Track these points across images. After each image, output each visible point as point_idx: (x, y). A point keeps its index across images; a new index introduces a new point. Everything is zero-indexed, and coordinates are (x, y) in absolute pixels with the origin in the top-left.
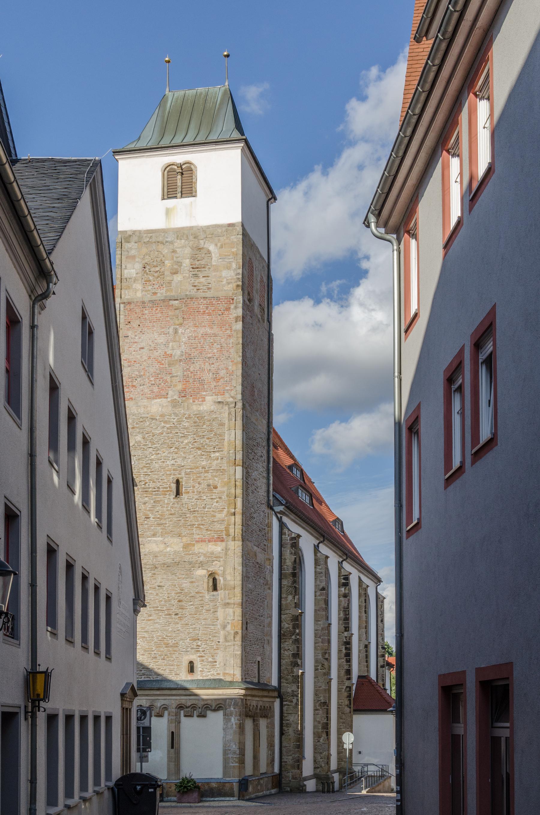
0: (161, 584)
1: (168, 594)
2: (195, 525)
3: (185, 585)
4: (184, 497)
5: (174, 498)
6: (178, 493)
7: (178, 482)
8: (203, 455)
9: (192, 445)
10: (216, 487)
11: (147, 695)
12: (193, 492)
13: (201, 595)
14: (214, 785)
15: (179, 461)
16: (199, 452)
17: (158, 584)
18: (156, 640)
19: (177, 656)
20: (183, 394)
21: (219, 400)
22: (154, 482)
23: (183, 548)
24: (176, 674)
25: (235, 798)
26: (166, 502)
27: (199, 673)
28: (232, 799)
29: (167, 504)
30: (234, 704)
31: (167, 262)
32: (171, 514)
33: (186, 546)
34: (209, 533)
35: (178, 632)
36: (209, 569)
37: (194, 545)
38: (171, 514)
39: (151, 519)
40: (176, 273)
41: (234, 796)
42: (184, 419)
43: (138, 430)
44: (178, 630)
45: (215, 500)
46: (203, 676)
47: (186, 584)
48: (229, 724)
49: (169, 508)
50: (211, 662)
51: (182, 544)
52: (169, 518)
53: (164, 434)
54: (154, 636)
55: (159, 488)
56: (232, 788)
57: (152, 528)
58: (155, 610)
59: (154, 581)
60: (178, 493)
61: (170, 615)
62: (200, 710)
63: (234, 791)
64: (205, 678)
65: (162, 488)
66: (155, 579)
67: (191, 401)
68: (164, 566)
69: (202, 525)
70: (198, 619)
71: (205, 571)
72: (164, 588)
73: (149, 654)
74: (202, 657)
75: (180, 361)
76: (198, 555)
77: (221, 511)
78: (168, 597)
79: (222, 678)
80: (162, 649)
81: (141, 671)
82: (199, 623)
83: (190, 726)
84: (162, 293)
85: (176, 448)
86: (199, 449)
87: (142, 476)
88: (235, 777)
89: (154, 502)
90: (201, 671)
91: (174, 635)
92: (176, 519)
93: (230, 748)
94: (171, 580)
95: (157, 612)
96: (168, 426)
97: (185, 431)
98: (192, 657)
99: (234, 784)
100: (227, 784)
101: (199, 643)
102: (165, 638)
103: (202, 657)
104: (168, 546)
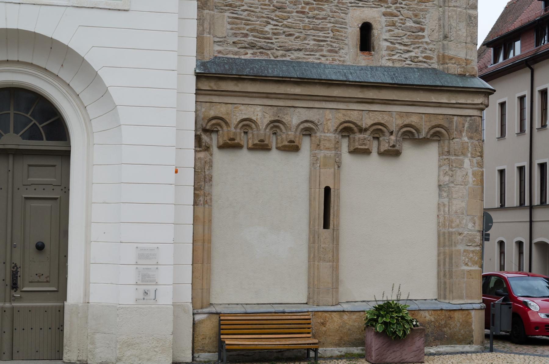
11: (268, 96)
14: (428, 317)
19: (334, 9)
24: (330, 51)
25: (474, 347)
27: (384, 53)
28: (467, 348)
30: (470, 127)
41: (471, 343)
46: (393, 61)
48: (459, 174)
50: (411, 30)
56: (467, 324)
62: (393, 138)
63: (471, 331)
64: (397, 65)
74: (392, 15)
79: (435, 66)
81: (246, 35)
83: (364, 180)
88: (472, 298)
90: (388, 48)
93: (460, 230)
98: (371, 14)
99: (473, 313)
100: (457, 315)
103: (392, 15)
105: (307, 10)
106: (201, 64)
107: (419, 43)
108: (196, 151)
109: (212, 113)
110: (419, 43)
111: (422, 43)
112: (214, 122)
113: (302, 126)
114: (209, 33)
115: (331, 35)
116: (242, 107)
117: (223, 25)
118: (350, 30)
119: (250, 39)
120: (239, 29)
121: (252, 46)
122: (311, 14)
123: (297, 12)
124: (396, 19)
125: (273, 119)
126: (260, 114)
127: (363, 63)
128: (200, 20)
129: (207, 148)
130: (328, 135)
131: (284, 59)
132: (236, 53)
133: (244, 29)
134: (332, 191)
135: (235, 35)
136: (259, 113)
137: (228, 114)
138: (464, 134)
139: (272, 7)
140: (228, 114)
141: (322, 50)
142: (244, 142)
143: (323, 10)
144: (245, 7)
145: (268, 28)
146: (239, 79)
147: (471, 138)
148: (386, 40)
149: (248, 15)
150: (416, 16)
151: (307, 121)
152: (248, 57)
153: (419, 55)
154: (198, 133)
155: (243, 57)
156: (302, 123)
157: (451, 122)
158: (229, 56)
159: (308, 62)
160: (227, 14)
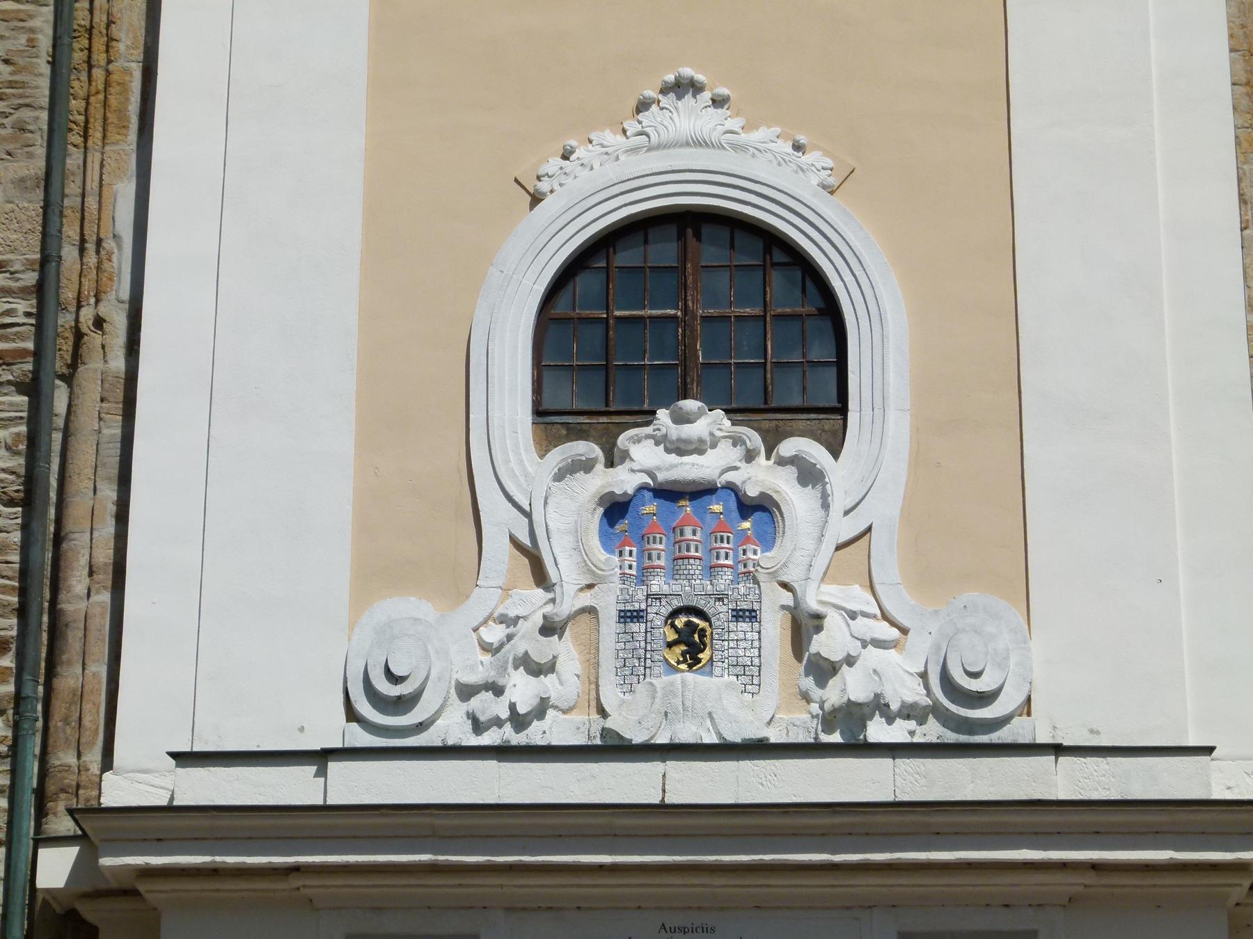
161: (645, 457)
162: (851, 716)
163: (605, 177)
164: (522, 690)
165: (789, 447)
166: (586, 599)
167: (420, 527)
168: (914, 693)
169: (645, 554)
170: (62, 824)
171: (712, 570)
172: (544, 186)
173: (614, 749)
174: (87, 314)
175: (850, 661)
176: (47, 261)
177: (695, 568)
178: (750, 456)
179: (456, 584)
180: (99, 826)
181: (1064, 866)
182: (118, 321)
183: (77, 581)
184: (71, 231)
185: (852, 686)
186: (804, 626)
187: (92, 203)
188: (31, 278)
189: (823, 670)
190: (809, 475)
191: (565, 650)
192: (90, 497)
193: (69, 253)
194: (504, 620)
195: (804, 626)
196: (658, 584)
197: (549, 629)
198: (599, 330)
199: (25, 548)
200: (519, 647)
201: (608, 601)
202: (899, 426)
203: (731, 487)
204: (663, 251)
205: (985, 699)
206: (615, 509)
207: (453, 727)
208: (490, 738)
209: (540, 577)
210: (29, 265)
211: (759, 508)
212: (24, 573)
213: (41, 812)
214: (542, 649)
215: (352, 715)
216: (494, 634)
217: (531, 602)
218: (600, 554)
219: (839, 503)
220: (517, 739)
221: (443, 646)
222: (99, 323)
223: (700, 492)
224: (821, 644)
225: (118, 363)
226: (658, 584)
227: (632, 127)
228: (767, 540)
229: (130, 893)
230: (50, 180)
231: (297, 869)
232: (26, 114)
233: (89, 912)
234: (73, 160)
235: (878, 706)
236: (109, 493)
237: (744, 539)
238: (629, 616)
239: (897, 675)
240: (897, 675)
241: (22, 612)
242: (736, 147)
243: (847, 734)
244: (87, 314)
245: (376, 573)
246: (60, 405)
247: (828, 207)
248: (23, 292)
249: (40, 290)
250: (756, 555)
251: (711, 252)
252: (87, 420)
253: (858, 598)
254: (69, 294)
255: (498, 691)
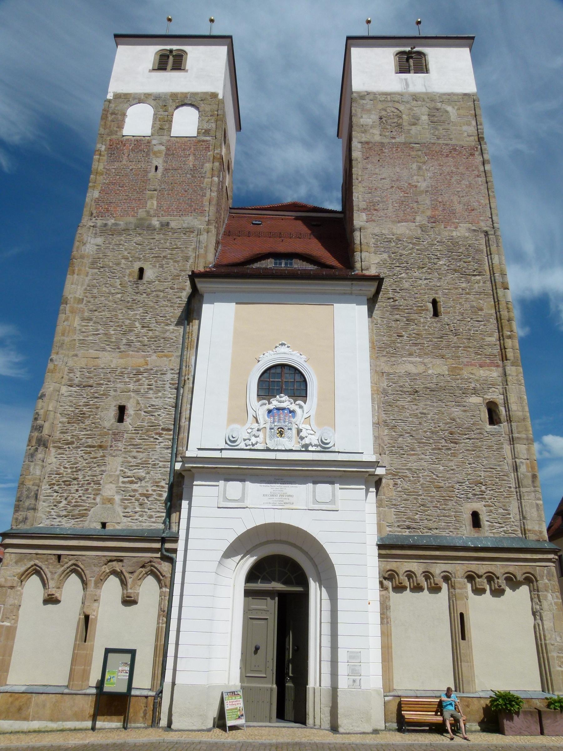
0: (425, 411)
1: (435, 423)
2: (460, 347)
3: (456, 413)
4: (444, 318)
5: (431, 318)
6: (436, 314)
7: (435, 303)
8: (462, 277)
9: (448, 266)
10: (481, 310)
12: (455, 313)
13: (478, 427)
15: (435, 282)
16: (456, 275)
17: (421, 410)
18: (422, 481)
20: (434, 220)
21: (474, 228)
22: (406, 300)
23: (448, 371)
26: (422, 320)
29: (423, 323)
31: (404, 116)
32: (429, 334)
33: (453, 370)
34: (479, 356)
35: (452, 472)
36: (485, 396)
37: (461, 369)
38: (429, 334)
39: (405, 338)
40: (414, 124)
42: (436, 243)
43: (383, 249)
44: (452, 470)
45: (482, 323)
47: (456, 412)
49: (427, 328)
51: (446, 366)
52: (428, 338)
53: (414, 254)
54: (420, 475)
55: (411, 306)
57: (407, 347)
58: (419, 443)
59: (415, 407)
60: (436, 314)
61: (439, 449)
65: (416, 306)
66: (416, 405)
67: (443, 227)
68: (426, 391)
69: (469, 347)
70: (479, 457)
71: (481, 399)
72: (429, 417)
73: (415, 499)
74: (489, 506)
75: (427, 191)
76: (468, 380)
77: (491, 336)
78: (435, 427)
80: (433, 494)
81: (405, 521)
82: (480, 461)
84: (401, 139)
85: (429, 269)
86: (455, 271)
87: (390, 293)
89: (407, 320)
90: (489, 526)
91: (448, 476)
92: (436, 340)
94: (437, 407)
95: (422, 445)
96: (417, 247)
97: (438, 253)
98: (478, 506)
101: (483, 488)
102: (436, 479)
103: (489, 506)
104: (429, 368)
105: (438, 505)
106: (381, 539)
107: (508, 522)
108: (380, 591)
109: (388, 568)
110: (508, 522)
111: (510, 522)
112: (389, 572)
113: (442, 575)
114: (383, 521)
115: (454, 519)
116: (405, 564)
117: (392, 517)
118: (465, 516)
119: (407, 523)
120: (401, 518)
121: (409, 528)
122: (441, 508)
123: (433, 507)
124: (492, 508)
125: (424, 570)
126: (416, 568)
127: (476, 535)
128: (379, 514)
129: (387, 589)
130: (459, 579)
131: (428, 534)
132: (400, 532)
133: (403, 518)
134: (465, 615)
135: (398, 521)
136: (416, 567)
137: (397, 568)
138: (545, 578)
139: (418, 505)
140: (397, 568)
141: (450, 528)
142: (407, 584)
143: (447, 505)
144: (403, 505)
145: (416, 517)
146: (402, 547)
147: (549, 580)
148: (487, 521)
149: (405, 510)
150: (504, 506)
151: (444, 572)
152: (407, 534)
153: (509, 529)
154: (381, 580)
155: (404, 534)
156: (442, 572)
157: (535, 570)
158: (396, 534)
159: (442, 536)
160: (393, 510)
161: (275, 403)
162: (306, 446)
163: (270, 358)
164: (254, 440)
165: (298, 402)
166: (264, 426)
167: (238, 414)
168: (316, 443)
169: (274, 419)
170: (179, 459)
171: (285, 422)
172: (260, 359)
173: (268, 450)
174: (186, 377)
175: (306, 437)
176: (180, 369)
177: (282, 421)
178: (291, 404)
179: (243, 422)
180: (185, 460)
181: (339, 471)
182: (191, 379)
183: (183, 420)
184: (184, 364)
185: (306, 441)
186: (299, 431)
187: (188, 360)
188: (178, 371)
189: (302, 438)
190: (301, 407)
191: (261, 434)
192: (186, 406)
193: (184, 368)
194: (251, 428)
195: (299, 431)
196: (276, 424)
197: (258, 430)
198: (267, 383)
199: (175, 414)
200: (253, 433)
201: (268, 426)
202: (315, 400)
203: (288, 408)
204: (279, 370)
205: (327, 444)
206: (270, 411)
207: (242, 446)
208: (248, 448)
209: (257, 422)
210: (178, 369)
211: (292, 412)
212: (175, 419)
213: (176, 457)
214: (257, 433)
215: (226, 443)
216: (249, 431)
217: (256, 426)
218: (267, 418)
219: (305, 412)
220: (253, 448)
221: (241, 433)
222: (188, 379)
223: (283, 409)
224: (302, 434)
225: (191, 385)
226: (276, 424)
227: (274, 350)
228: (294, 417)
229: (190, 470)
230: (182, 356)
231: (217, 467)
232: (178, 345)
233: (183, 473)
234: (185, 353)
235: (311, 444)
236: (189, 406)
237: (290, 417)
238: (271, 429)
239: (314, 440)
240: (314, 440)
241: (174, 425)
242: (291, 354)
243: (306, 449)
244: (186, 377)
245: (231, 420)
246: (181, 392)
247: (305, 364)
248: (176, 374)
249: (179, 373)
250: (292, 419)
251: (286, 370)
252: (186, 394)
253: (308, 427)
254: (184, 374)
255: (250, 440)
